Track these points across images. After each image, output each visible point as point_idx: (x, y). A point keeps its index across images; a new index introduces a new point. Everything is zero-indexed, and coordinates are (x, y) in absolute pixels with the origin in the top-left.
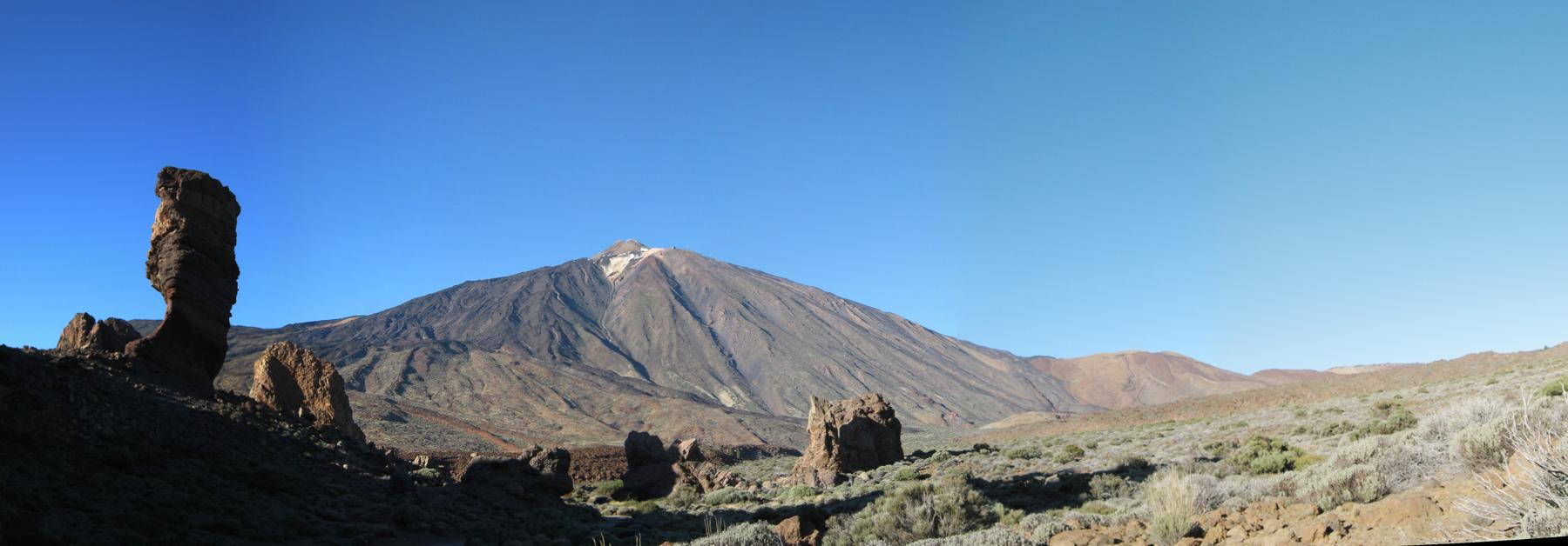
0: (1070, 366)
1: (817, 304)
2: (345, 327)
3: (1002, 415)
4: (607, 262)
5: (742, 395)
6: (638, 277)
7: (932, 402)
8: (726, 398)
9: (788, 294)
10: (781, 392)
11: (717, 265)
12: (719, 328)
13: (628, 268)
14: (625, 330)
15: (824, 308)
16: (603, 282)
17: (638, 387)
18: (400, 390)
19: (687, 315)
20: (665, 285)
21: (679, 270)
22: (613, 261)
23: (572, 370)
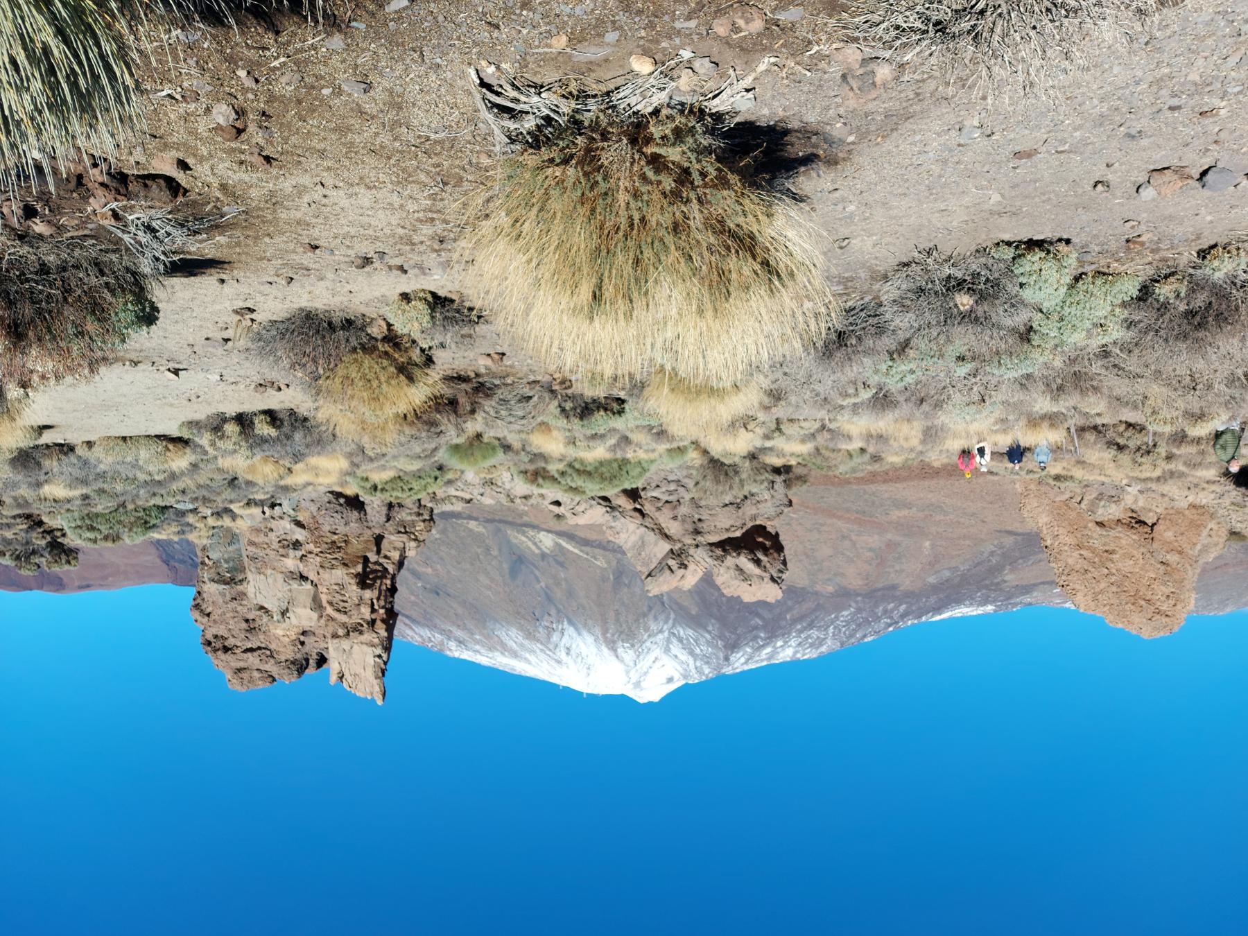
8: (547, 541)
10: (488, 549)
14: (650, 609)
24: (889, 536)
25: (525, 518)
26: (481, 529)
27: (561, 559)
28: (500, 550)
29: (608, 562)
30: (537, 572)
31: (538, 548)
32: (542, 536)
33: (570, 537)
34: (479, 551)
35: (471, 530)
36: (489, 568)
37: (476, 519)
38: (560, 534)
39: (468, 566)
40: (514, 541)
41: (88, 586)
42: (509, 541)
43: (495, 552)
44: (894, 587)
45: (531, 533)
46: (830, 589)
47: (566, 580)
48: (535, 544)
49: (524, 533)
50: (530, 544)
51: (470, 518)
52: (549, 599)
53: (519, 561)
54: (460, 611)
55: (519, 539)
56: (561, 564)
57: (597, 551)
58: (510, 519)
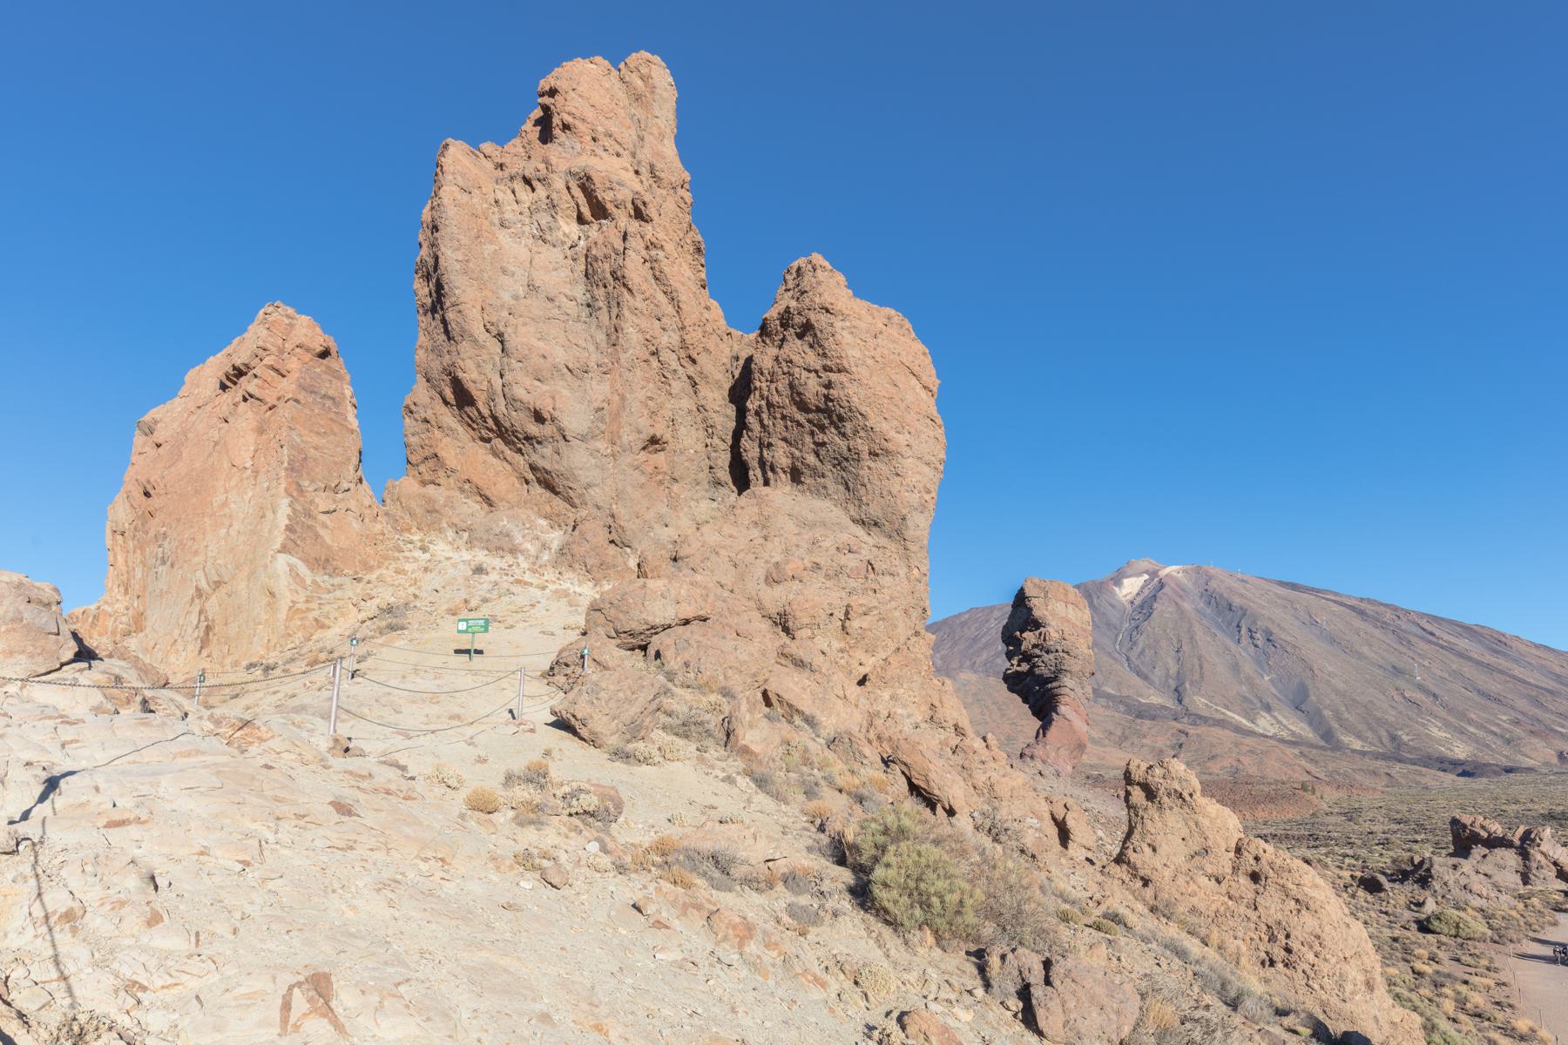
4: (1118, 583)
8: (1264, 724)
9: (1335, 608)
22: (1126, 581)
28: (1322, 716)
30: (1273, 690)
32: (1272, 731)
33: (1238, 729)
35: (1359, 736)
36: (1333, 696)
37: (1354, 751)
38: (1251, 733)
40: (1305, 726)
42: (1310, 724)
43: (1327, 713)
45: (1284, 734)
47: (1241, 683)
48: (1279, 722)
49: (1293, 734)
50: (1285, 722)
51: (1363, 754)
52: (1258, 662)
53: (1299, 702)
54: (1365, 650)
55: (1302, 729)
56: (1245, 699)
57: (1206, 714)
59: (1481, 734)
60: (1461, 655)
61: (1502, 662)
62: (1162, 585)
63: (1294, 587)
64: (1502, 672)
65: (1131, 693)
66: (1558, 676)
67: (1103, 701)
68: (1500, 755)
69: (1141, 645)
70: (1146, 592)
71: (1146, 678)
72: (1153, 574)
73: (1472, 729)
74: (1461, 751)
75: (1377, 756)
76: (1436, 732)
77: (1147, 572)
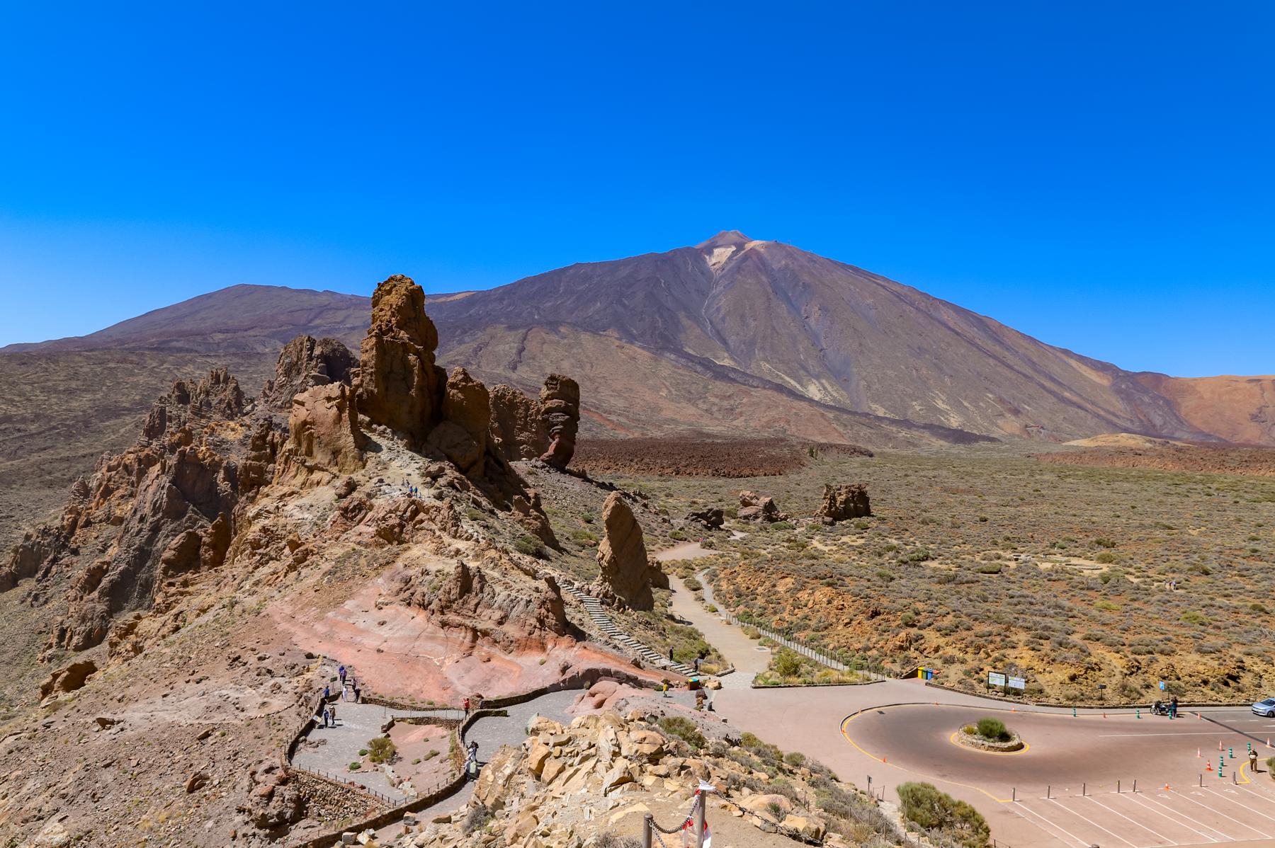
0: (1185, 388)
1: (912, 305)
2: (460, 302)
3: (1092, 433)
5: (829, 388)
6: (738, 269)
7: (1016, 412)
8: (814, 391)
9: (882, 292)
11: (812, 260)
12: (812, 322)
13: (730, 258)
14: (723, 319)
15: (917, 309)
16: (705, 272)
17: (732, 375)
18: (514, 368)
19: (782, 309)
20: (764, 278)
21: (778, 263)
22: (716, 251)
23: (673, 356)
24: (514, 376)
25: (831, 416)
26: (874, 406)
27: (802, 372)
29: (759, 366)
31: (822, 385)
34: (877, 386)
37: (878, 418)
38: (802, 398)
39: (889, 372)
41: (1250, 381)
44: (511, 328)
46: (562, 330)
48: (825, 388)
49: (834, 399)
50: (829, 388)
58: (845, 416)
59: (971, 408)
60: (971, 342)
61: (997, 349)
62: (746, 257)
63: (856, 270)
64: (995, 358)
65: (708, 355)
66: (1034, 363)
67: (683, 361)
68: (979, 425)
69: (723, 312)
70: (733, 263)
71: (724, 342)
72: (740, 246)
73: (966, 404)
74: (955, 422)
75: (893, 422)
76: (941, 405)
77: (735, 244)
